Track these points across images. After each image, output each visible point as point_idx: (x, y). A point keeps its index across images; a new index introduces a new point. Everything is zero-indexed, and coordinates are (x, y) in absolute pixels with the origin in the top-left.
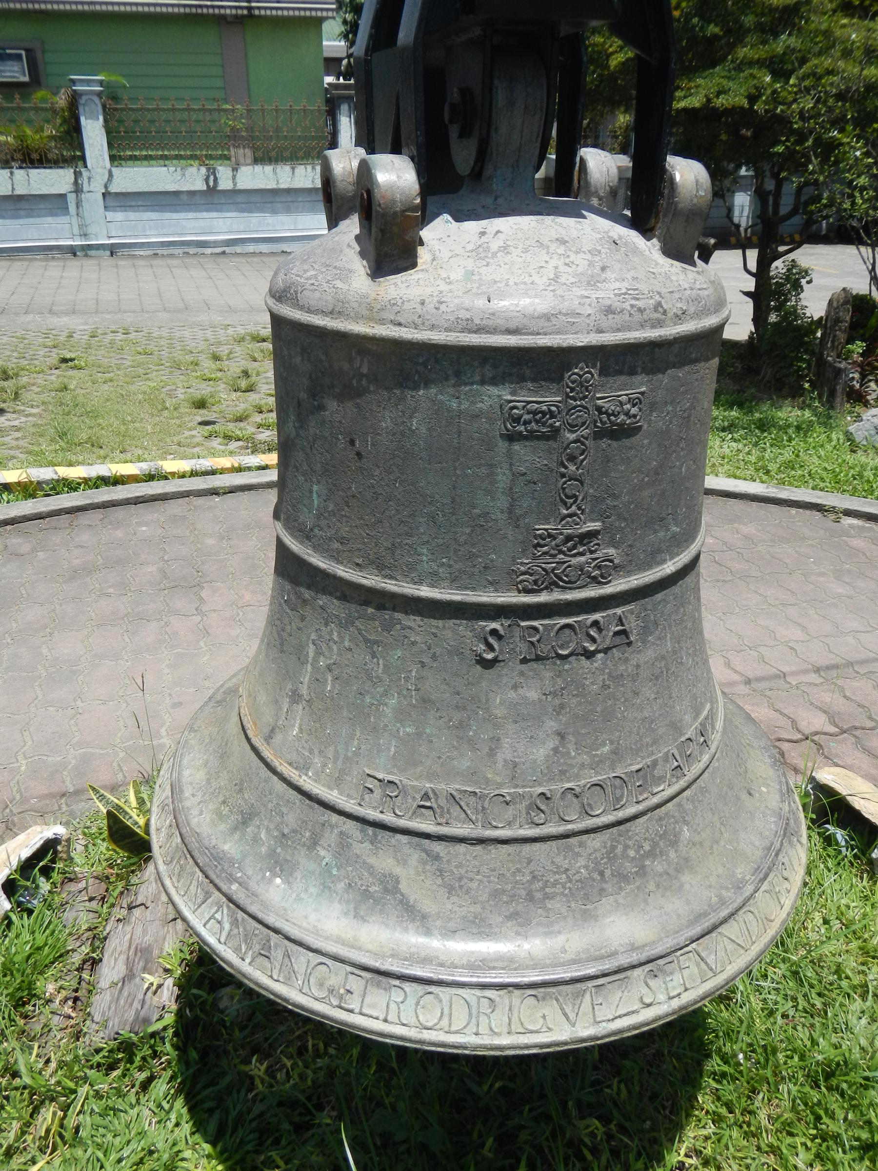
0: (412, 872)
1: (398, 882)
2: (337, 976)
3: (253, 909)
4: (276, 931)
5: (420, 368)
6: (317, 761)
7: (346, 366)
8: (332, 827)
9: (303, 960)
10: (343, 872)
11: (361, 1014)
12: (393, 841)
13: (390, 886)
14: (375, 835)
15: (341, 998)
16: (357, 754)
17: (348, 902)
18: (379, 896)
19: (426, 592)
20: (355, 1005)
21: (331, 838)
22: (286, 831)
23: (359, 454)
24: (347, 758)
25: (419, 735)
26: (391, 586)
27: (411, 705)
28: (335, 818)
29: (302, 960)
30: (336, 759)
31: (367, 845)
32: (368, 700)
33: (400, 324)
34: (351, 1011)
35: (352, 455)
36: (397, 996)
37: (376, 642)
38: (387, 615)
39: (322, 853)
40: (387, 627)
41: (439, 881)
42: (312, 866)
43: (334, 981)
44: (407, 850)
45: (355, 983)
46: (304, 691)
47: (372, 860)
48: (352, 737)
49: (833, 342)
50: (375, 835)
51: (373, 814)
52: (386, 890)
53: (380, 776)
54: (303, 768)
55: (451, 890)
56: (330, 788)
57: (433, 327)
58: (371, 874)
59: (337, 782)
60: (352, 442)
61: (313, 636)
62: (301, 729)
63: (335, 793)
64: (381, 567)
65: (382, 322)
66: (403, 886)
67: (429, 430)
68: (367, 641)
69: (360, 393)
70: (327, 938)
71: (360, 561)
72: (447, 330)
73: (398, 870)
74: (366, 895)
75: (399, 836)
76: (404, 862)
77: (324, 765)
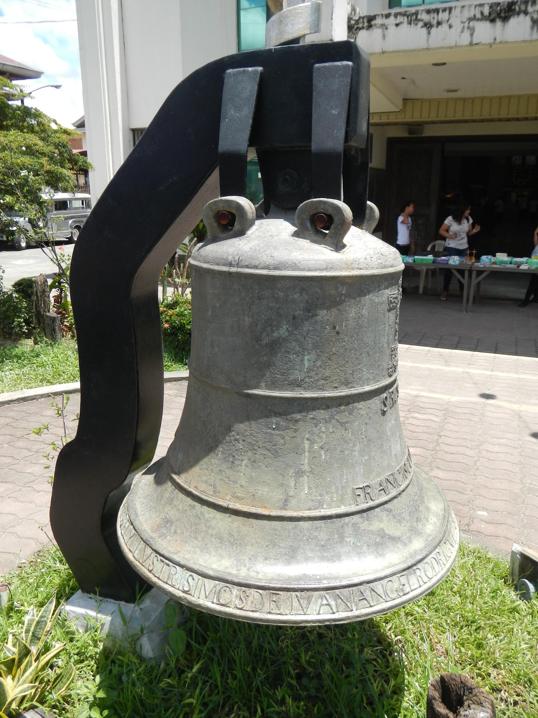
0: (386, 523)
1: (384, 531)
2: (396, 582)
3: (344, 583)
4: (361, 584)
5: (367, 286)
6: (327, 498)
7: (333, 292)
8: (347, 524)
9: (380, 587)
10: (362, 542)
11: (412, 591)
12: (375, 513)
13: (382, 534)
14: (367, 515)
15: (402, 590)
16: (346, 482)
17: (372, 552)
18: (383, 541)
19: (367, 388)
20: (407, 589)
21: (349, 530)
22: (323, 543)
23: (338, 333)
24: (343, 487)
25: (370, 458)
26: (354, 391)
27: (365, 445)
28: (347, 519)
29: (378, 587)
30: (337, 491)
31: (366, 522)
32: (346, 452)
33: (361, 269)
34: (408, 593)
35: (334, 334)
36: (418, 573)
37: (347, 422)
38: (350, 406)
39: (348, 540)
40: (350, 414)
41: (395, 521)
42: (347, 549)
43: (396, 585)
44: (381, 514)
45: (403, 580)
46: (306, 468)
47: (371, 528)
48: (342, 476)
49: (44, 304)
50: (367, 515)
51: (365, 506)
52: (382, 537)
53: (361, 486)
54: (320, 505)
55: (400, 522)
56: (339, 507)
57: (372, 268)
58: (373, 534)
59: (342, 501)
60: (334, 328)
61: (307, 436)
62: (310, 488)
63: (343, 507)
64: (347, 384)
65: (353, 269)
66: (387, 531)
67: (369, 313)
68: (341, 424)
69: (341, 303)
70: (383, 570)
71: (336, 385)
72: (377, 268)
73: (382, 526)
74: (377, 544)
75: (376, 510)
76: (381, 521)
77: (332, 497)
